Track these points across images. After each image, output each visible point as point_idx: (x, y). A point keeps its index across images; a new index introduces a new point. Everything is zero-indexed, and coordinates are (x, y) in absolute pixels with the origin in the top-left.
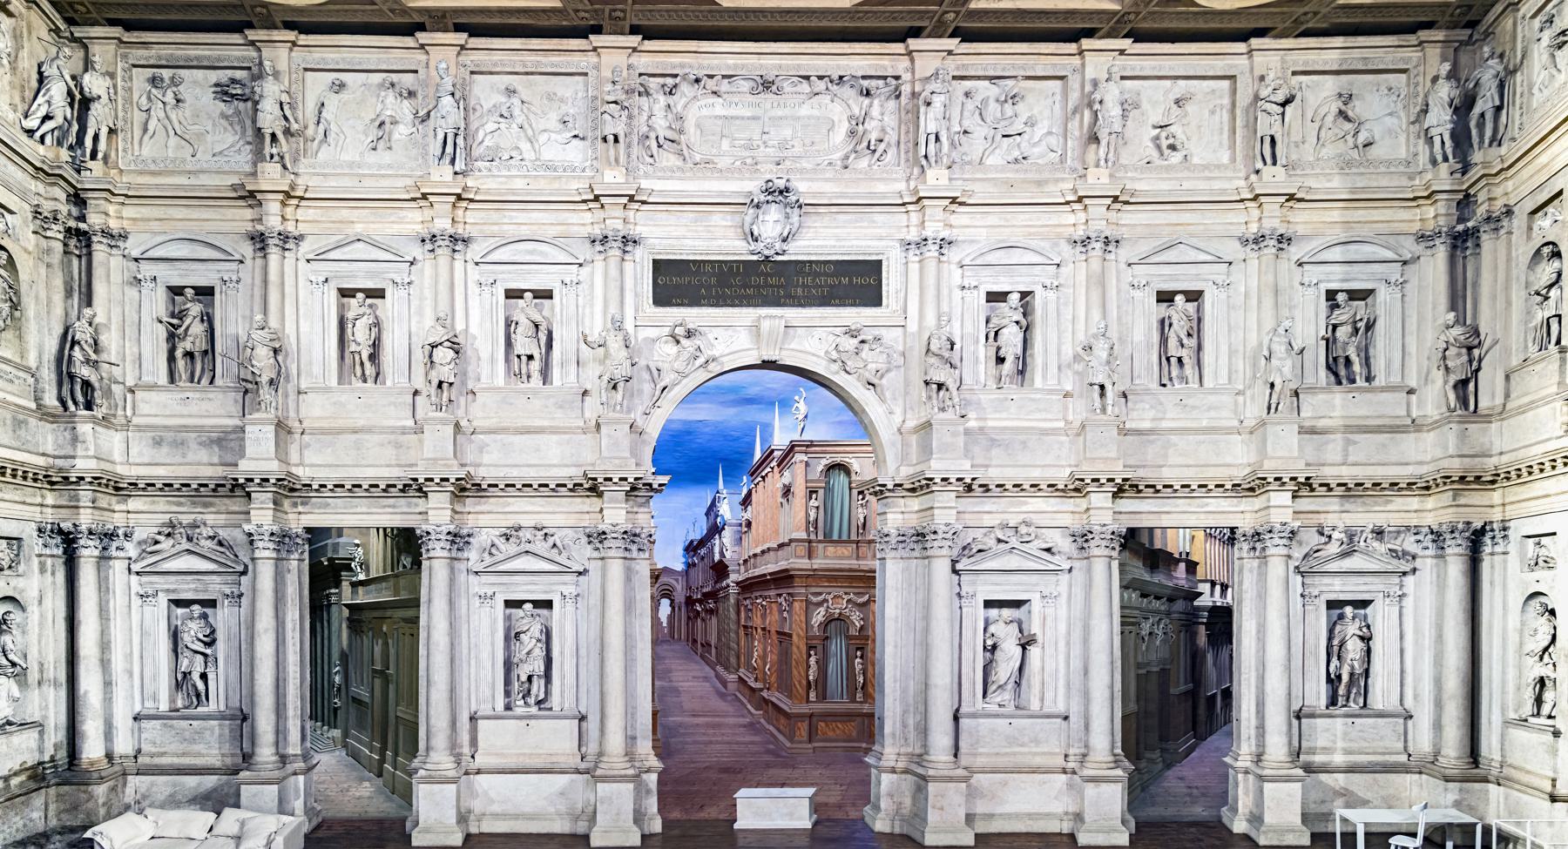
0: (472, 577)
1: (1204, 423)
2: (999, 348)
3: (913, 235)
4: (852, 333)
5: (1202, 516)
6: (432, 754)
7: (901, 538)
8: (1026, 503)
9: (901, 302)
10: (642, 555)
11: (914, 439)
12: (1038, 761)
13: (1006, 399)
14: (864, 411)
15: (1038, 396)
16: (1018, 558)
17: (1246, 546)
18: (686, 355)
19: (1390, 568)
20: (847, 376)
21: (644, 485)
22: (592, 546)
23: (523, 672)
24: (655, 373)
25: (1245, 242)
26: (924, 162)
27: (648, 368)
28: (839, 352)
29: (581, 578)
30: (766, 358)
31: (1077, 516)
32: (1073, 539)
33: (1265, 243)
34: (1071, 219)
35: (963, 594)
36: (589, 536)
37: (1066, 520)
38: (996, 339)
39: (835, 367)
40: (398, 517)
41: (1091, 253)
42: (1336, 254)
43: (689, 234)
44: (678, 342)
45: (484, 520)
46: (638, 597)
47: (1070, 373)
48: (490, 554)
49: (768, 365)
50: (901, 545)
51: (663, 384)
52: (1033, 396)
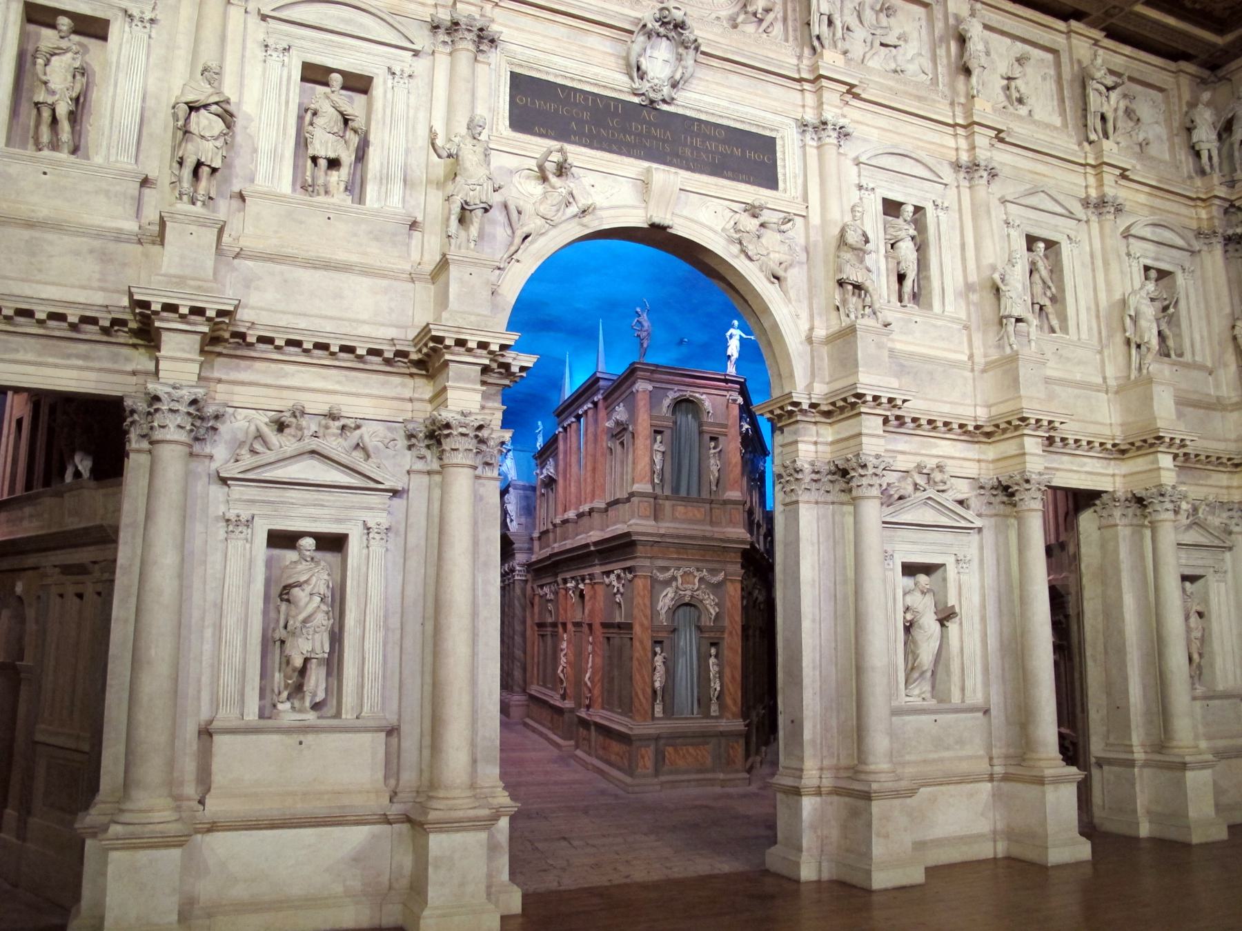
0: (217, 491)
1: (1078, 377)
3: (810, 116)
4: (753, 211)
5: (1083, 476)
6: (137, 794)
7: (815, 477)
8: (936, 446)
9: (800, 188)
11: (824, 350)
12: (965, 767)
13: (910, 321)
14: (766, 310)
15: (939, 323)
16: (932, 511)
17: (1117, 513)
18: (555, 198)
19: (1216, 543)
20: (747, 262)
22: (415, 452)
23: (299, 649)
24: (514, 214)
25: (1086, 203)
26: (816, 43)
27: (506, 207)
29: (396, 501)
30: (657, 220)
31: (983, 465)
32: (982, 492)
33: (1108, 209)
34: (951, 142)
36: (411, 436)
37: (972, 470)
40: (93, 376)
41: (976, 182)
42: (1147, 232)
43: (558, 50)
44: (544, 179)
45: (241, 396)
47: (963, 303)
48: (253, 452)
49: (656, 236)
50: (814, 486)
51: (526, 230)
52: (933, 321)
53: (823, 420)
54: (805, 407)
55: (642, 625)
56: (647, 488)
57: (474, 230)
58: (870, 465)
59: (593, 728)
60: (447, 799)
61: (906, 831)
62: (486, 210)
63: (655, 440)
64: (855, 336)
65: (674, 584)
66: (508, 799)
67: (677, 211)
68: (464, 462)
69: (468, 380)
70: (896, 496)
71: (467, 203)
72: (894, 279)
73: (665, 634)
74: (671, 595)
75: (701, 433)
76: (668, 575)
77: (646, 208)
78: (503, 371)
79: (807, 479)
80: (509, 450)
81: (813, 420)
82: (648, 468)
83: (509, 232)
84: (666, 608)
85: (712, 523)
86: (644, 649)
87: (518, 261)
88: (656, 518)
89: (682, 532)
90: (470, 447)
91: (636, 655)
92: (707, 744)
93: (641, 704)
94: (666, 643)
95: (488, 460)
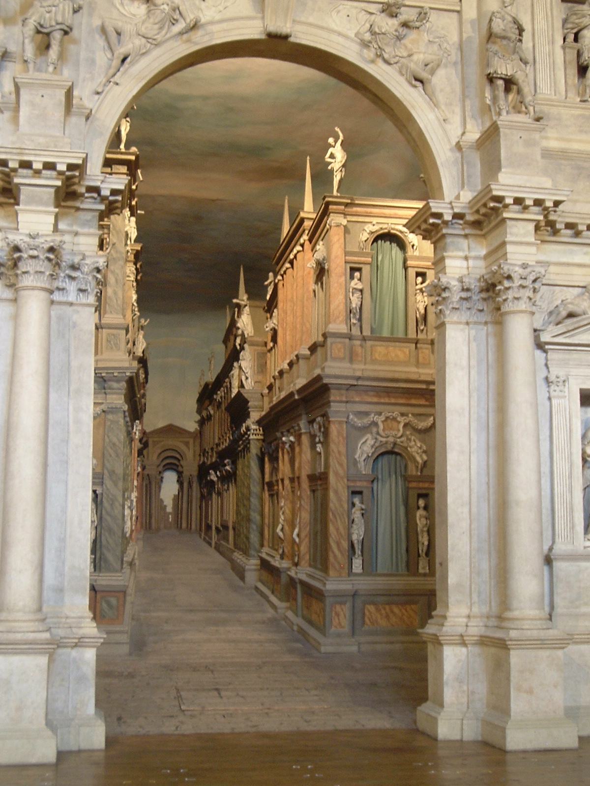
2: (579, 54)
10: (83, 299)
18: (158, 15)
20: (385, 66)
21: (90, 189)
24: (113, 36)
27: (103, 30)
28: (373, 33)
30: (273, 28)
35: (552, 378)
38: (576, 39)
39: (370, 54)
46: (74, 364)
50: (466, 304)
51: (121, 51)
53: (479, 232)
54: (448, 217)
55: (336, 474)
56: (343, 328)
57: (53, 53)
58: (515, 276)
59: (299, 586)
60: (8, 621)
61: (555, 686)
62: (66, 33)
63: (352, 278)
64: (499, 135)
65: (374, 430)
66: (96, 630)
67: (298, 19)
68: (35, 284)
69: (40, 202)
70: (564, 313)
71: (42, 26)
72: (573, 71)
73: (365, 484)
74: (371, 442)
75: (406, 268)
76: (366, 421)
77: (263, 18)
78: (95, 195)
79: (456, 298)
80: (246, 306)
81: (463, 233)
82: (342, 307)
83: (109, 55)
84: (365, 456)
85: (418, 364)
86: (339, 500)
87: (117, 84)
88: (351, 361)
89: (382, 375)
90: (42, 270)
91: (331, 505)
92: (415, 603)
93: (335, 556)
94: (366, 493)
95: (83, 287)
